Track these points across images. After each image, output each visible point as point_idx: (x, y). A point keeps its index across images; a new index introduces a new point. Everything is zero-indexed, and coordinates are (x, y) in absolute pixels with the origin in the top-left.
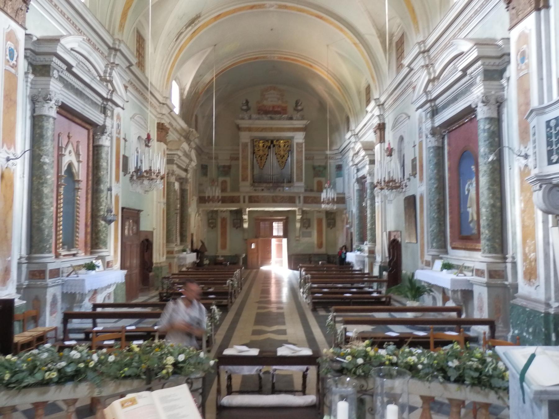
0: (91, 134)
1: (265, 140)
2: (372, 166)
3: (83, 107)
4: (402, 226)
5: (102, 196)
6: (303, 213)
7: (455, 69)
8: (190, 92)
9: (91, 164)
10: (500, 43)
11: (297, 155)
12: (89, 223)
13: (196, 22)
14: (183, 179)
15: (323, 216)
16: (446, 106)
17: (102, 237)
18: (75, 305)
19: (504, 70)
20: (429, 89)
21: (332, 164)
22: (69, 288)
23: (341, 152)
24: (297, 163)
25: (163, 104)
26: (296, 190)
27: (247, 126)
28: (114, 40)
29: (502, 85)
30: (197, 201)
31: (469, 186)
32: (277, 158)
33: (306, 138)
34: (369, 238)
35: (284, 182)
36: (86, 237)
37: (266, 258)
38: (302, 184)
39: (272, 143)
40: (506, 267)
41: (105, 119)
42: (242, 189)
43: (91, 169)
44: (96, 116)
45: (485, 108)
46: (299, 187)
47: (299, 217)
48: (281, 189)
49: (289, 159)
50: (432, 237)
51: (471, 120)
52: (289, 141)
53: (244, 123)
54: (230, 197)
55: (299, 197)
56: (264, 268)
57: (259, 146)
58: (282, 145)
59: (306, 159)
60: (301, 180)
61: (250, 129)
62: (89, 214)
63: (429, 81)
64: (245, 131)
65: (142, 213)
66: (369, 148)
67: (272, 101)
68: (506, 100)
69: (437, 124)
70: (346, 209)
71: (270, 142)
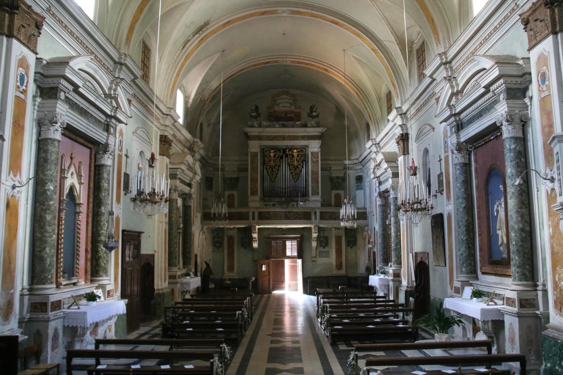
0: (93, 153)
1: (276, 149)
2: (396, 179)
3: (87, 126)
4: (430, 249)
5: (103, 219)
6: (320, 230)
7: (477, 84)
8: (195, 100)
9: (92, 185)
10: (521, 62)
11: (312, 166)
12: (89, 249)
13: (203, 30)
14: (186, 194)
15: (343, 233)
16: (471, 121)
17: (102, 264)
18: (76, 339)
19: (526, 89)
20: (453, 102)
21: (352, 174)
22: (71, 321)
23: (361, 163)
24: (312, 174)
25: (167, 115)
26: (311, 205)
27: (257, 134)
28: (120, 54)
29: (526, 104)
31: (498, 207)
32: (290, 169)
33: (322, 147)
34: (393, 259)
35: (298, 196)
36: (86, 264)
37: (279, 282)
38: (318, 198)
39: (284, 153)
40: (537, 295)
41: (108, 137)
42: (251, 204)
43: (92, 191)
44: (98, 134)
45: (510, 127)
46: (315, 202)
47: (315, 235)
48: (295, 204)
49: (304, 170)
50: (462, 261)
51: (497, 137)
52: (303, 150)
53: (254, 131)
55: (315, 213)
56: (276, 292)
57: (270, 156)
58: (295, 154)
59: (322, 169)
61: (259, 138)
62: (90, 239)
63: (453, 95)
64: (254, 140)
65: (142, 235)
66: (391, 159)
67: (284, 107)
68: (531, 118)
69: (462, 140)
70: (367, 226)
71: (282, 151)
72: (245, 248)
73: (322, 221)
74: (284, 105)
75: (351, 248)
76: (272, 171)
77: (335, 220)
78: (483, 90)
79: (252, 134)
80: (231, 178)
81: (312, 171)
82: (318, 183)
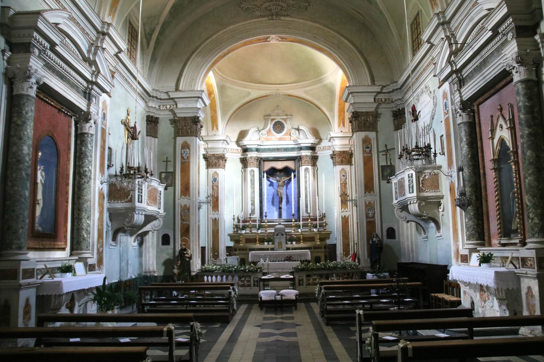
28: (103, 23)
44: (80, 102)
45: (522, 69)
69: (465, 98)
78: (490, 33)
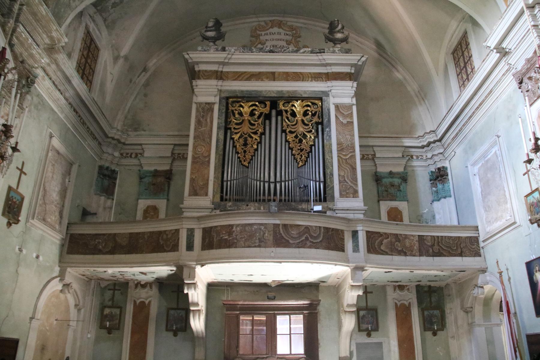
11: (338, 133)
15: (411, 297)
23: (440, 140)
27: (214, 68)
30: (62, 246)
32: (286, 141)
33: (358, 95)
38: (358, 203)
39: (274, 106)
46: (350, 206)
47: (351, 296)
54: (152, 233)
55: (355, 234)
57: (241, 114)
60: (355, 194)
61: (220, 76)
71: (268, 103)
72: (175, 335)
73: (373, 256)
74: (275, 43)
75: (435, 334)
76: (245, 144)
77: (405, 254)
79: (203, 67)
80: (156, 171)
81: (339, 144)
82: (354, 169)
